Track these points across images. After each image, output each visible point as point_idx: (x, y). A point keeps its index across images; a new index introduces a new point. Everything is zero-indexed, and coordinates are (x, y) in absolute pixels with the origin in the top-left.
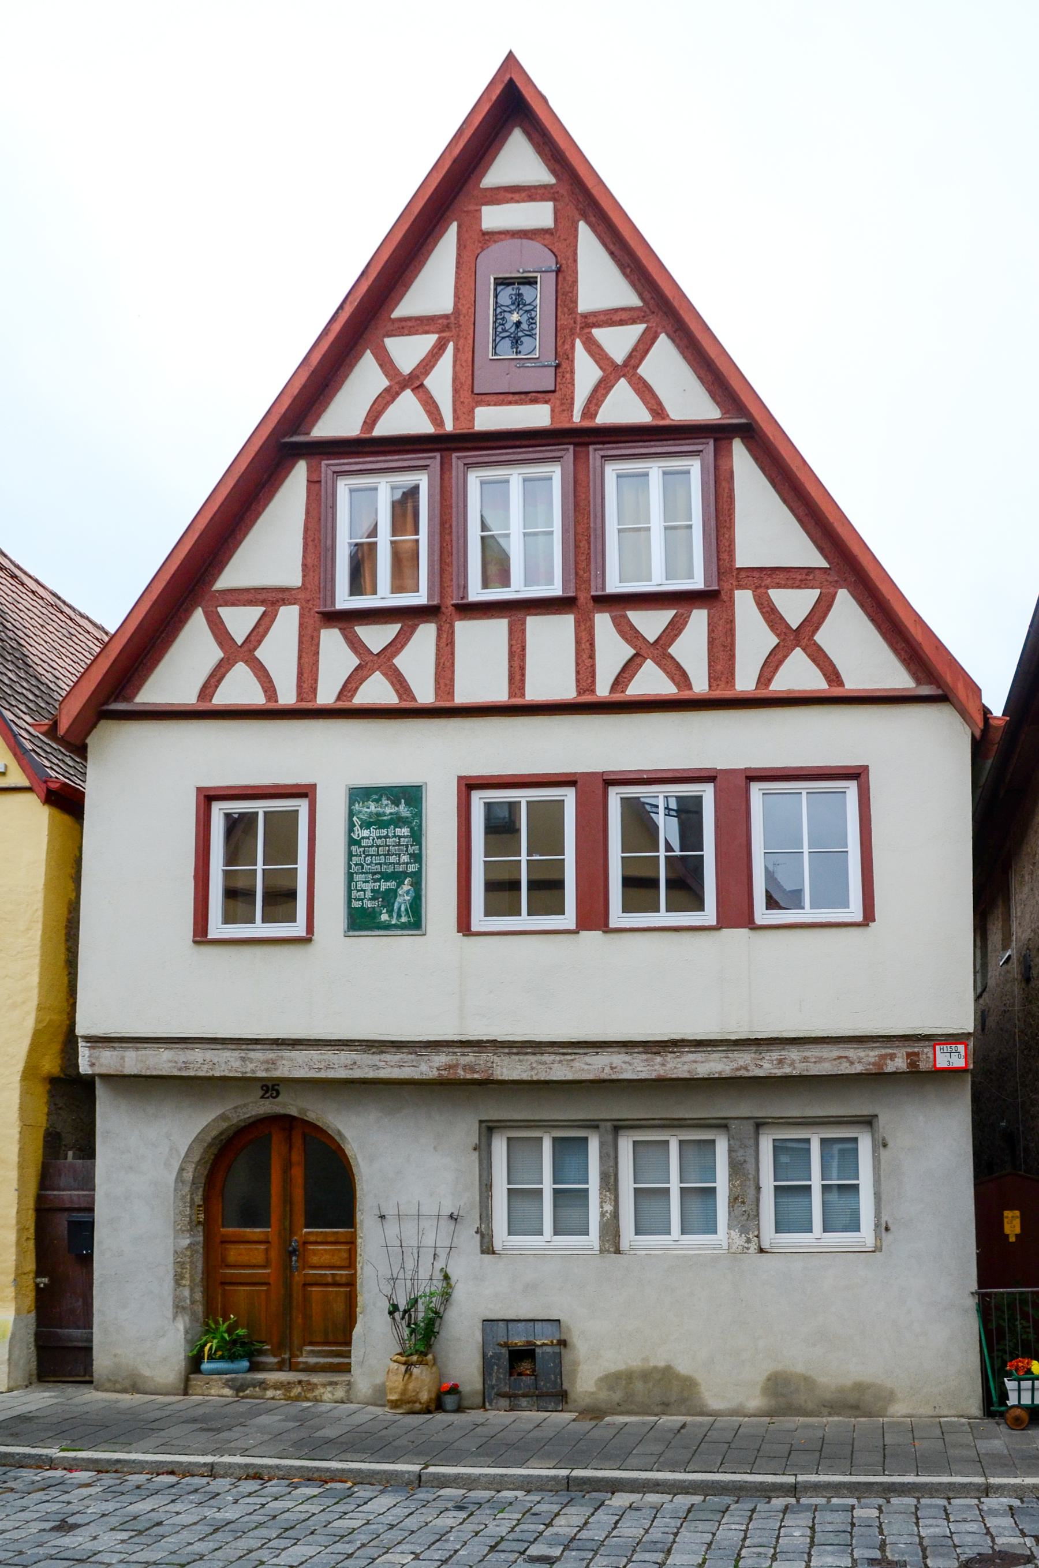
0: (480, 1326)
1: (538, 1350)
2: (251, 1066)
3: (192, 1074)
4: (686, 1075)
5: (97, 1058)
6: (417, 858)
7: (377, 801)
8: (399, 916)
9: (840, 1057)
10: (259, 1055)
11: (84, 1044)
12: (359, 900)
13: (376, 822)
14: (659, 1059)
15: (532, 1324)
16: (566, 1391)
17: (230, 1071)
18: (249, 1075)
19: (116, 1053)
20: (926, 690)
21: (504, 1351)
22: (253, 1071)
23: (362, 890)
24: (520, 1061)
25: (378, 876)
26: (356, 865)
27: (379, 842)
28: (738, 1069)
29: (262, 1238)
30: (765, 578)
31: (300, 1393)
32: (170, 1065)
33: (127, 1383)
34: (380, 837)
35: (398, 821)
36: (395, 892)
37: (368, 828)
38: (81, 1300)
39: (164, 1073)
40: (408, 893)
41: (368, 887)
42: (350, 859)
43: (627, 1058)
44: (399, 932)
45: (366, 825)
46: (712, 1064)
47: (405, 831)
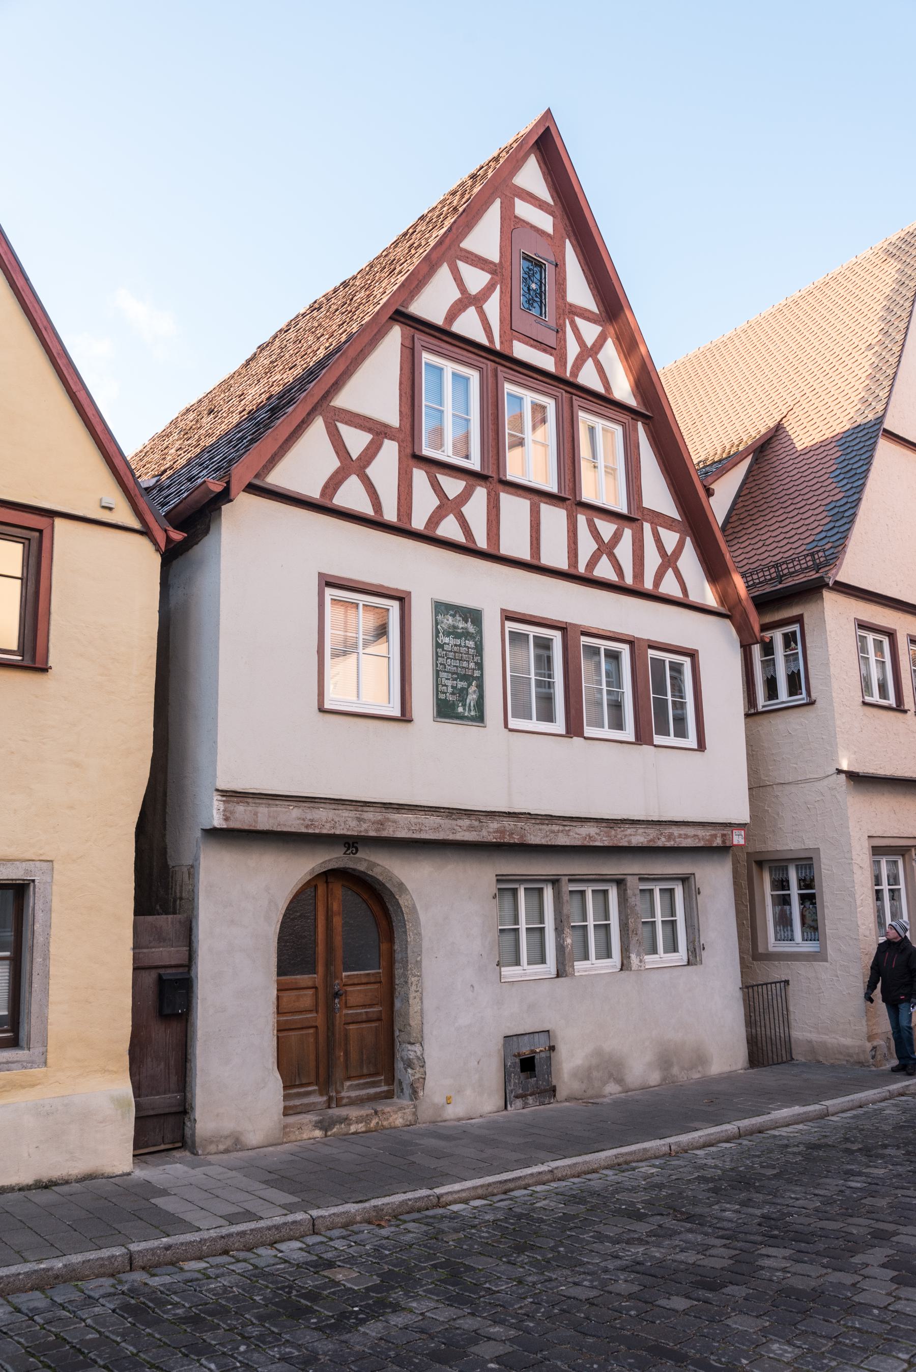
0: (502, 1042)
1: (537, 1057)
2: (365, 826)
3: (317, 831)
4: (626, 844)
5: (232, 812)
6: (480, 666)
7: (454, 616)
8: (470, 710)
9: (695, 835)
10: (371, 815)
11: (220, 798)
12: (444, 693)
13: (452, 632)
14: (613, 832)
15: (532, 1036)
16: (555, 1086)
17: (348, 830)
18: (363, 834)
19: (250, 808)
20: (722, 610)
21: (518, 1060)
22: (366, 831)
23: (445, 685)
24: (540, 830)
25: (455, 676)
26: (441, 664)
27: (455, 649)
28: (650, 841)
29: (310, 984)
30: (657, 519)
31: (378, 1123)
32: (298, 822)
33: (229, 1142)
34: (456, 645)
35: (466, 635)
36: (467, 689)
37: (448, 636)
38: (162, 1065)
39: (293, 830)
40: (475, 691)
41: (449, 683)
42: (437, 660)
43: (597, 831)
44: (470, 723)
45: (448, 634)
46: (639, 837)
47: (471, 644)
